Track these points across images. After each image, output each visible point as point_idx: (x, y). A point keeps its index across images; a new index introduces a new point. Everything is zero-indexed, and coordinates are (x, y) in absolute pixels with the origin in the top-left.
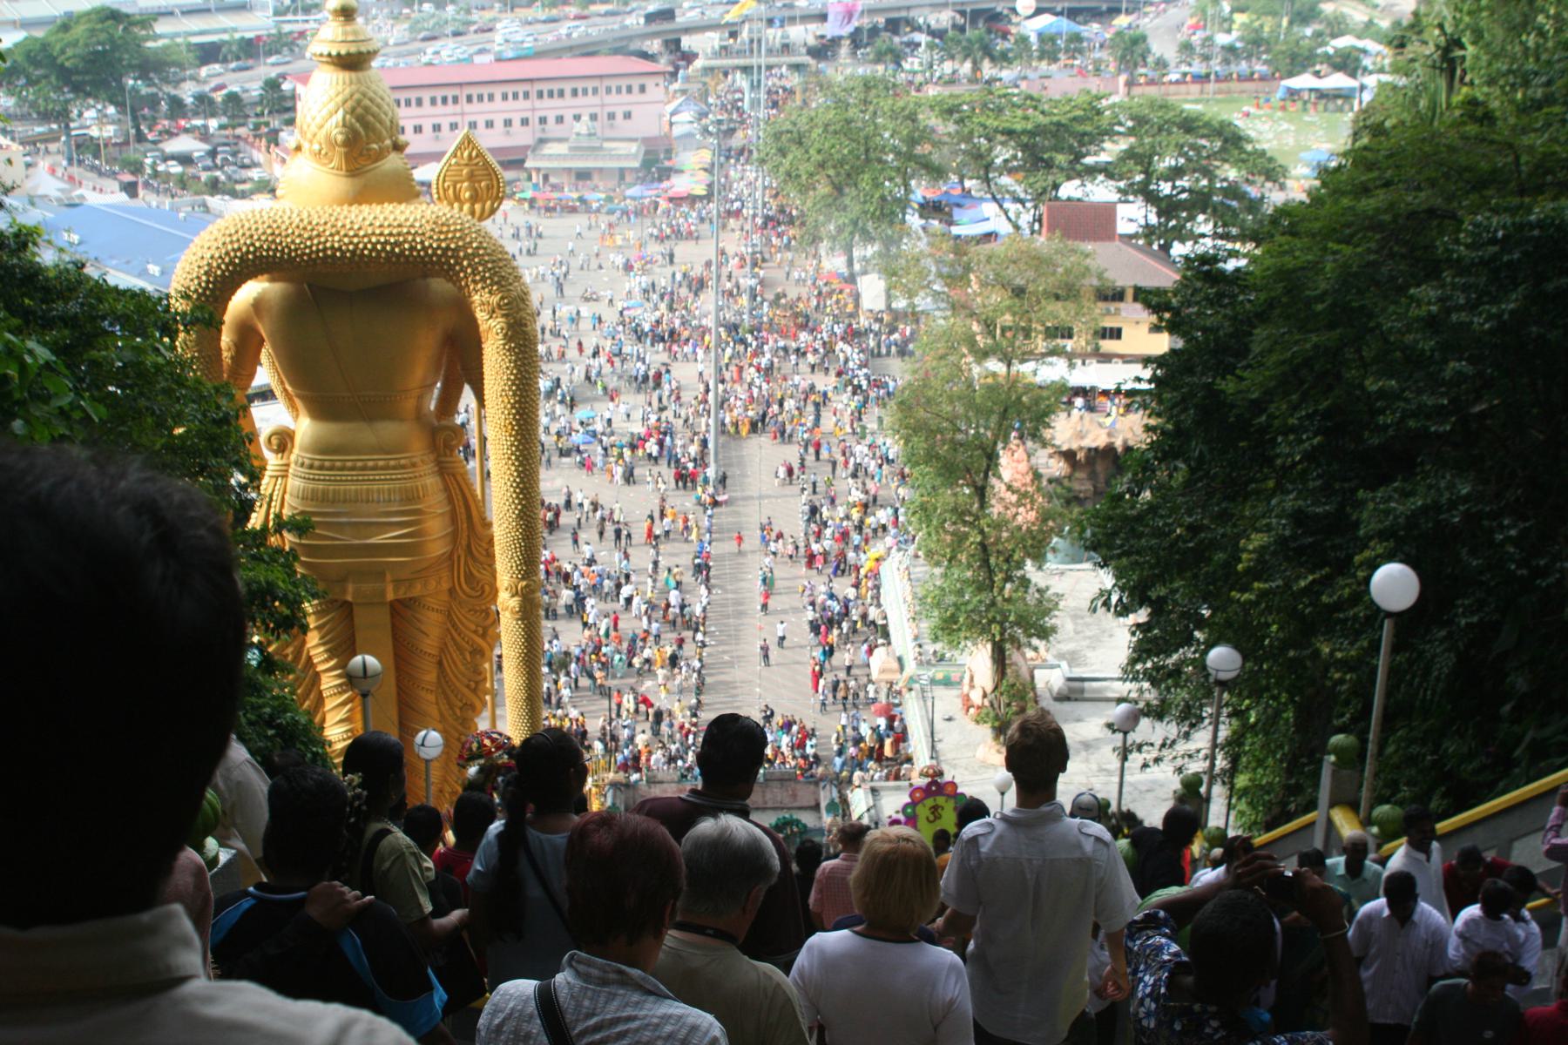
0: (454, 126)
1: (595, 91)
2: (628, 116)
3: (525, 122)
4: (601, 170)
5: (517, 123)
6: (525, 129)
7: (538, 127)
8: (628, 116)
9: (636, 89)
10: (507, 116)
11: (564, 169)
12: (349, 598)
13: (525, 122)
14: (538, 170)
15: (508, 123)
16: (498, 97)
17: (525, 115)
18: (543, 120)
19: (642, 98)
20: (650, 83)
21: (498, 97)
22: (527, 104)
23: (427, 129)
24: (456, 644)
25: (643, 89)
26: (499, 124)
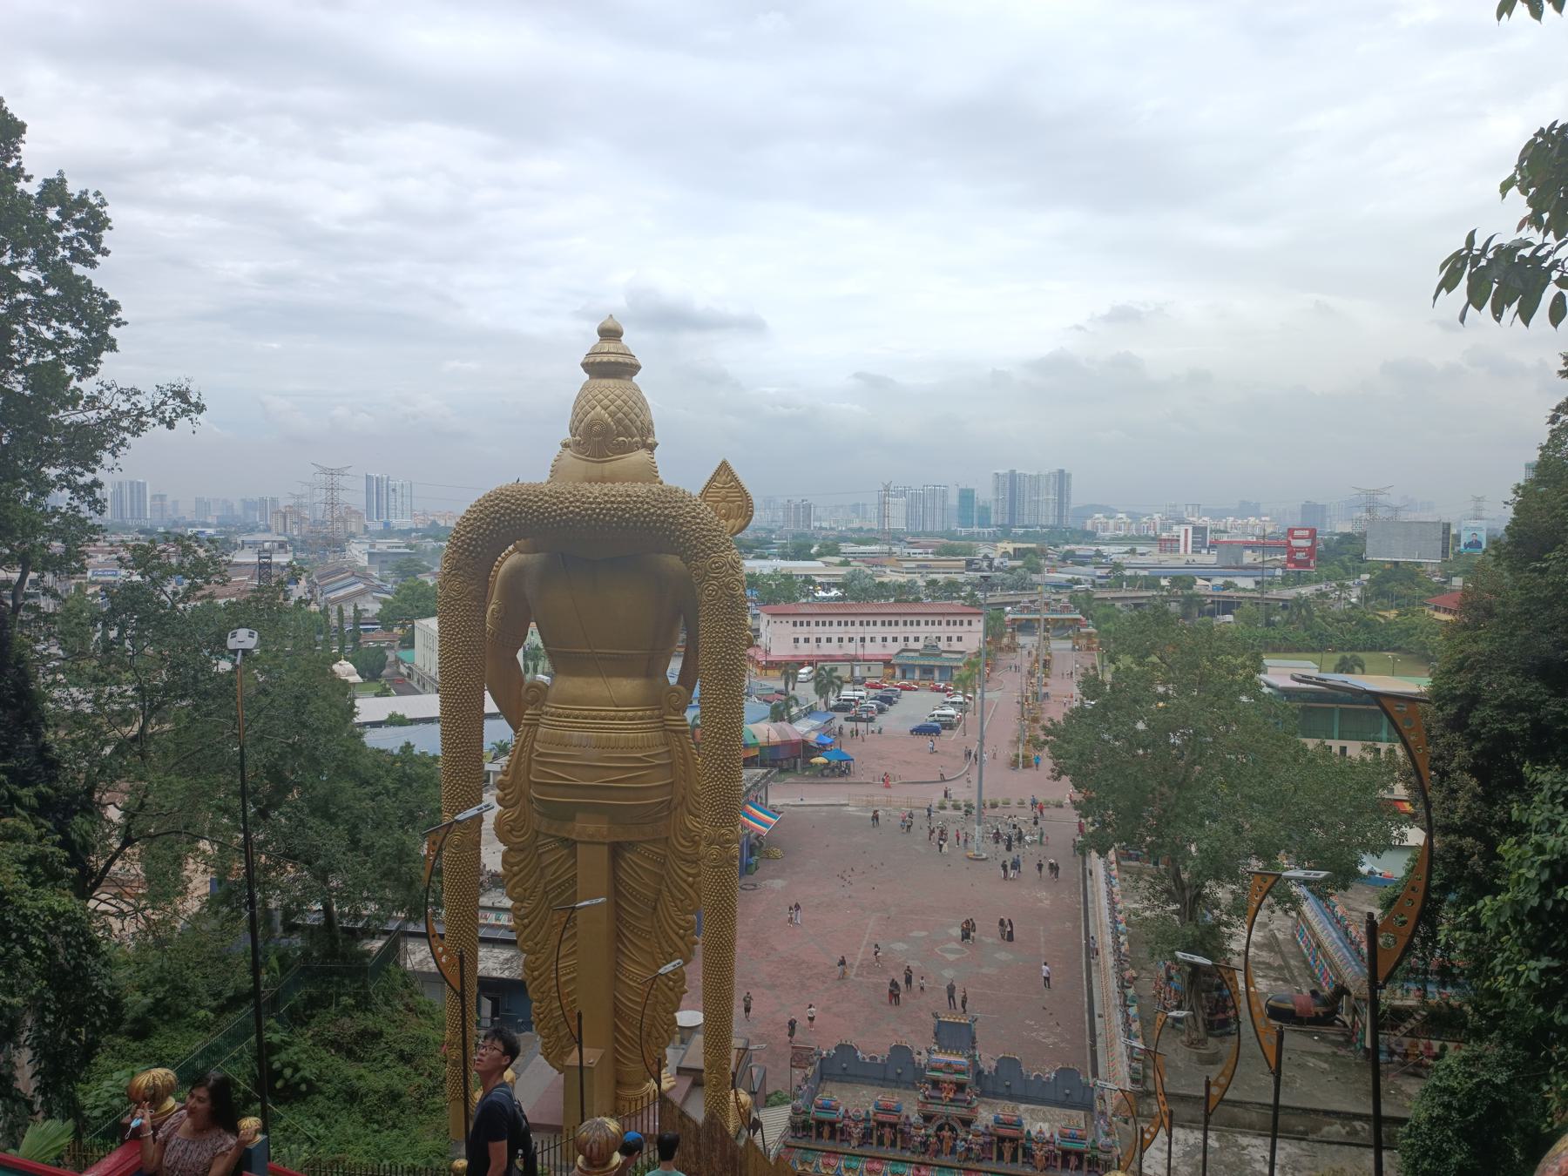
0: (851, 640)
1: (940, 623)
2: (960, 639)
5: (890, 639)
8: (960, 639)
9: (966, 623)
12: (574, 837)
13: (895, 639)
15: (884, 639)
18: (906, 639)
19: (969, 628)
20: (974, 619)
23: (835, 640)
24: (670, 891)
25: (970, 623)
26: (879, 640)
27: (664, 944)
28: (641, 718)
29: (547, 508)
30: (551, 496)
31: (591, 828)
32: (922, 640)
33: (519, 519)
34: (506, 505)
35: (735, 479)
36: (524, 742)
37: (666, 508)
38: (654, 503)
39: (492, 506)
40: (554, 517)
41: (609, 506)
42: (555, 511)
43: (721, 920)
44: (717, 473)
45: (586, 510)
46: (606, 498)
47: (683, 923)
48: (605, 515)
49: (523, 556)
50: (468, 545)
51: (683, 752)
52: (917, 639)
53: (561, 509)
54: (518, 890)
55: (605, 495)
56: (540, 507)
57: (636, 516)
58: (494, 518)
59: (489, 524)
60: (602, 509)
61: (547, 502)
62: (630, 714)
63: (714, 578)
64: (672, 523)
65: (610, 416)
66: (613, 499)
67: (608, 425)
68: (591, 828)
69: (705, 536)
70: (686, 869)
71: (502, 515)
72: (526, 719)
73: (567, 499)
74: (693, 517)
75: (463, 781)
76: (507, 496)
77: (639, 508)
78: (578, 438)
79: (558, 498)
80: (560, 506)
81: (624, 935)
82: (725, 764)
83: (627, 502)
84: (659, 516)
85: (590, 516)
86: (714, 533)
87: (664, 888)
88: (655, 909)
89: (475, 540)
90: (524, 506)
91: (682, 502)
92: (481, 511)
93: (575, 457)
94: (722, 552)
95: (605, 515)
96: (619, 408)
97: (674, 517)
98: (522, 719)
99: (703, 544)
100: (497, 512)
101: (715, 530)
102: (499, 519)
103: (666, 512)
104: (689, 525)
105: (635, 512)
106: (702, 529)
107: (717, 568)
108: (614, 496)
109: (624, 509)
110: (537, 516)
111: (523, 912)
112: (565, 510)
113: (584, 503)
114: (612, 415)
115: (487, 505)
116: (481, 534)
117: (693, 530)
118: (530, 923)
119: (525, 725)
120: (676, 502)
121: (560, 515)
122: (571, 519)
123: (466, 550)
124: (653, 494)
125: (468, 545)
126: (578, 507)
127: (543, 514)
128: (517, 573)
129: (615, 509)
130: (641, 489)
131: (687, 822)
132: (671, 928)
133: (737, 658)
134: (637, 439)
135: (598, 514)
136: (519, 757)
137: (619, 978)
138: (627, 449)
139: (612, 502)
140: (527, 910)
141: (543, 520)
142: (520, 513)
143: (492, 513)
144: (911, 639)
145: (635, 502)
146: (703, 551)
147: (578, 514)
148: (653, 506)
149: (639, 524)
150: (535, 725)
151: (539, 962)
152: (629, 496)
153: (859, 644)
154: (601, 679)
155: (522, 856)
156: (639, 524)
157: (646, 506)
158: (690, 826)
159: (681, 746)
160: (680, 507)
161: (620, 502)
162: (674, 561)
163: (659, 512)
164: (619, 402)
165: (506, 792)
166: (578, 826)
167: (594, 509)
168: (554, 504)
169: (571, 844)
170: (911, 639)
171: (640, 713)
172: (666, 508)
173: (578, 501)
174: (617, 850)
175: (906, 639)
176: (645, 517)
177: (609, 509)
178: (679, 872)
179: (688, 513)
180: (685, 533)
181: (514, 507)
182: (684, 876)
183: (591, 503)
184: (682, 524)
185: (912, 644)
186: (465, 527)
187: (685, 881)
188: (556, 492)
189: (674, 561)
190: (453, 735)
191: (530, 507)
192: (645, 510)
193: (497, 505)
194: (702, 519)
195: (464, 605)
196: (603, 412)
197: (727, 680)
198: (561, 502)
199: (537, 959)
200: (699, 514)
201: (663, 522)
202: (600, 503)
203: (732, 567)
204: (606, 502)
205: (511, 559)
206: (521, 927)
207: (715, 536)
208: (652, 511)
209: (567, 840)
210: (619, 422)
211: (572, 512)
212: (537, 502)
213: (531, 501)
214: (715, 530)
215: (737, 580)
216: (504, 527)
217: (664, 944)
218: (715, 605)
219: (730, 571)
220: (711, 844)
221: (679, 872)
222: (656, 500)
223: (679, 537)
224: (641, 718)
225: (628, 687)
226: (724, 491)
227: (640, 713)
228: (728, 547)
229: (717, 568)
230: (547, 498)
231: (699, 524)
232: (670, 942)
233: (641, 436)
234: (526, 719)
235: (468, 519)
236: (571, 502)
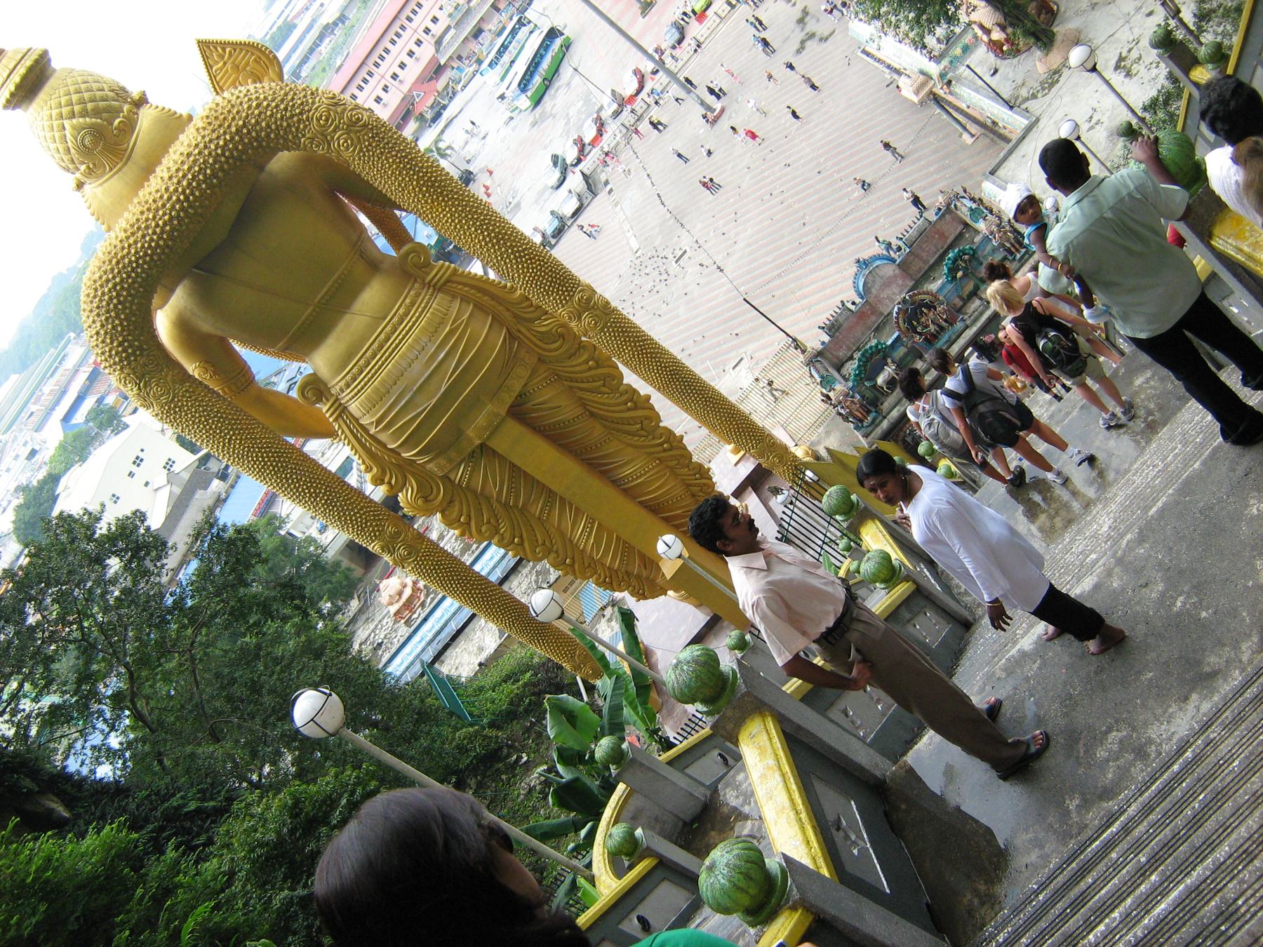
0: (385, 89)
3: (419, 43)
4: (482, 19)
5: (415, 48)
6: (423, 46)
7: (428, 37)
10: (406, 50)
11: (463, 42)
12: (478, 442)
13: (419, 43)
14: (451, 58)
15: (411, 54)
16: (390, 46)
17: (414, 39)
21: (390, 46)
22: (409, 32)
26: (407, 60)
27: (627, 428)
28: (413, 304)
29: (143, 246)
30: (133, 234)
31: (481, 420)
32: (439, 14)
33: (134, 282)
34: (110, 285)
35: (223, 45)
36: (352, 432)
37: (229, 126)
38: (214, 136)
39: (101, 301)
40: (158, 246)
41: (185, 183)
42: (152, 240)
43: (651, 357)
44: (205, 58)
45: (173, 207)
46: (175, 180)
47: (625, 397)
48: (192, 194)
49: (167, 307)
50: (125, 350)
51: (473, 287)
52: (435, 20)
53: (154, 233)
54: (483, 529)
55: (170, 178)
56: (137, 252)
57: (215, 162)
58: (115, 306)
59: (117, 316)
60: (184, 192)
61: (136, 242)
62: (401, 311)
63: (335, 131)
64: (249, 132)
65: (83, 116)
66: (181, 174)
67: (92, 126)
68: (481, 420)
69: (286, 109)
70: (580, 360)
71: (118, 295)
72: (331, 416)
73: (147, 220)
74: (258, 106)
75: (352, 510)
76: (101, 277)
77: (210, 154)
78: (83, 167)
79: (139, 228)
80: (150, 231)
81: (594, 459)
82: (518, 251)
83: (195, 161)
84: (232, 138)
85: (182, 208)
86: (289, 97)
87: (580, 394)
88: (592, 415)
89: (124, 341)
90: (124, 267)
91: (233, 106)
92: (98, 315)
93: (101, 185)
94: (313, 103)
95: (192, 194)
96: (82, 102)
97: (244, 125)
98: (328, 419)
99: (292, 116)
100: (111, 299)
101: (286, 94)
102: (120, 302)
103: (233, 129)
104: (263, 116)
105: (211, 161)
106: (277, 106)
107: (327, 120)
108: (177, 170)
109: (201, 169)
110: (145, 262)
111: (507, 536)
112: (158, 230)
113: (164, 206)
114: (84, 114)
115: (95, 305)
116: (123, 330)
117: (271, 116)
118: (521, 537)
119: (336, 420)
120: (229, 112)
121: (160, 238)
122: (172, 230)
123: (127, 358)
124: (204, 129)
125: (125, 350)
126: (164, 214)
127: (146, 254)
128: (184, 327)
129: (194, 177)
130: (187, 141)
131: (539, 329)
132: (621, 412)
133: (428, 167)
134: (126, 107)
135: (187, 199)
136: (363, 446)
137: (629, 488)
138: (130, 125)
139: (184, 176)
140: (509, 531)
141: (152, 259)
142: (129, 277)
143: (108, 304)
144: (431, 25)
145: (200, 153)
146: (299, 121)
147: (171, 218)
148: (218, 138)
149: (226, 166)
150: (343, 411)
151: (561, 551)
152: (189, 155)
153: (396, 83)
154: (347, 317)
155: (457, 508)
156: (226, 166)
157: (213, 147)
158: (543, 329)
159: (465, 285)
160: (238, 112)
161: (189, 169)
162: (282, 161)
163: (228, 137)
164: (75, 97)
165: (386, 480)
166: (470, 433)
167: (178, 199)
168: (144, 236)
169: (484, 449)
170: (431, 25)
171: (408, 301)
172: (229, 126)
173: (157, 210)
174: (519, 412)
175: (427, 31)
176: (223, 154)
177: (189, 184)
178: (578, 369)
179: (249, 107)
180: (268, 126)
181: (118, 280)
182: (585, 367)
183: (169, 199)
184: (257, 123)
185: (437, 29)
186: (103, 342)
187: (590, 369)
188: (132, 226)
189: (282, 161)
190: (303, 490)
191: (130, 262)
192: (216, 149)
193: (103, 294)
194: (265, 98)
195: (183, 396)
196: (74, 121)
197: (442, 192)
198: (147, 228)
199: (556, 552)
200: (257, 98)
201: (241, 139)
202: (176, 190)
203: (336, 104)
204: (179, 182)
205: (164, 323)
206: (519, 547)
207: (293, 99)
208: (221, 143)
209: (473, 452)
210: (97, 113)
211: (165, 224)
212: (129, 253)
213: (123, 257)
214: (286, 94)
215: (352, 110)
216: (132, 303)
217: (627, 428)
218: (361, 150)
219: (339, 110)
220: (580, 318)
221: (578, 369)
222: (213, 131)
223: (268, 135)
224: (413, 304)
225: (372, 296)
226: (229, 66)
227: (408, 301)
228: (312, 94)
229: (327, 120)
230: (131, 241)
231: (268, 105)
232: (632, 422)
233: (126, 102)
234: (331, 416)
235: (98, 333)
236: (154, 217)
